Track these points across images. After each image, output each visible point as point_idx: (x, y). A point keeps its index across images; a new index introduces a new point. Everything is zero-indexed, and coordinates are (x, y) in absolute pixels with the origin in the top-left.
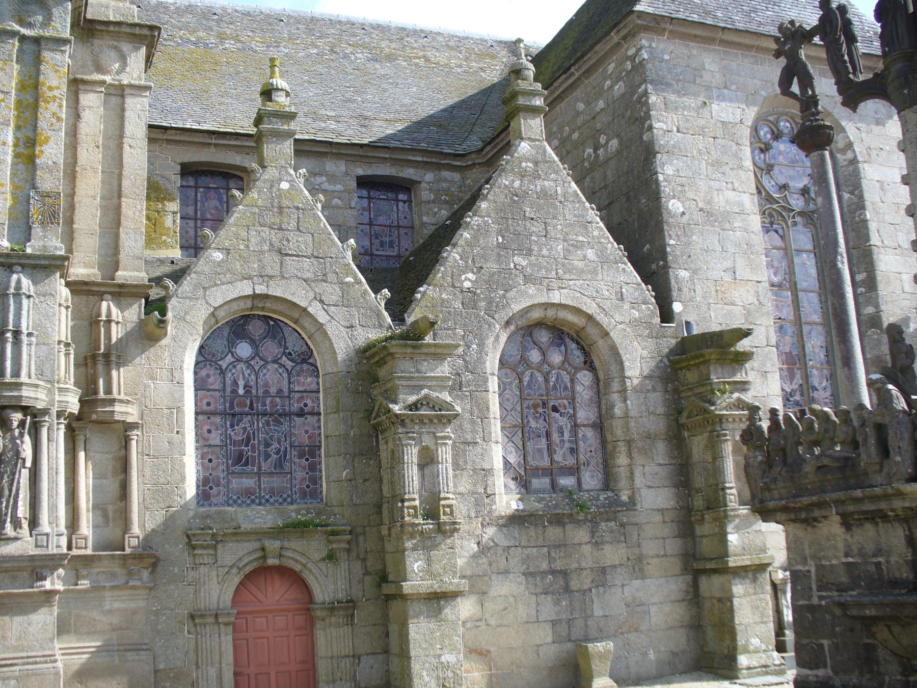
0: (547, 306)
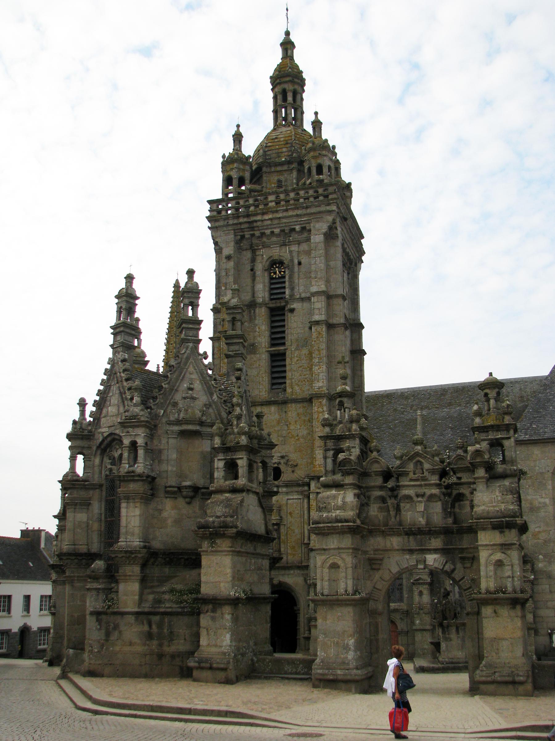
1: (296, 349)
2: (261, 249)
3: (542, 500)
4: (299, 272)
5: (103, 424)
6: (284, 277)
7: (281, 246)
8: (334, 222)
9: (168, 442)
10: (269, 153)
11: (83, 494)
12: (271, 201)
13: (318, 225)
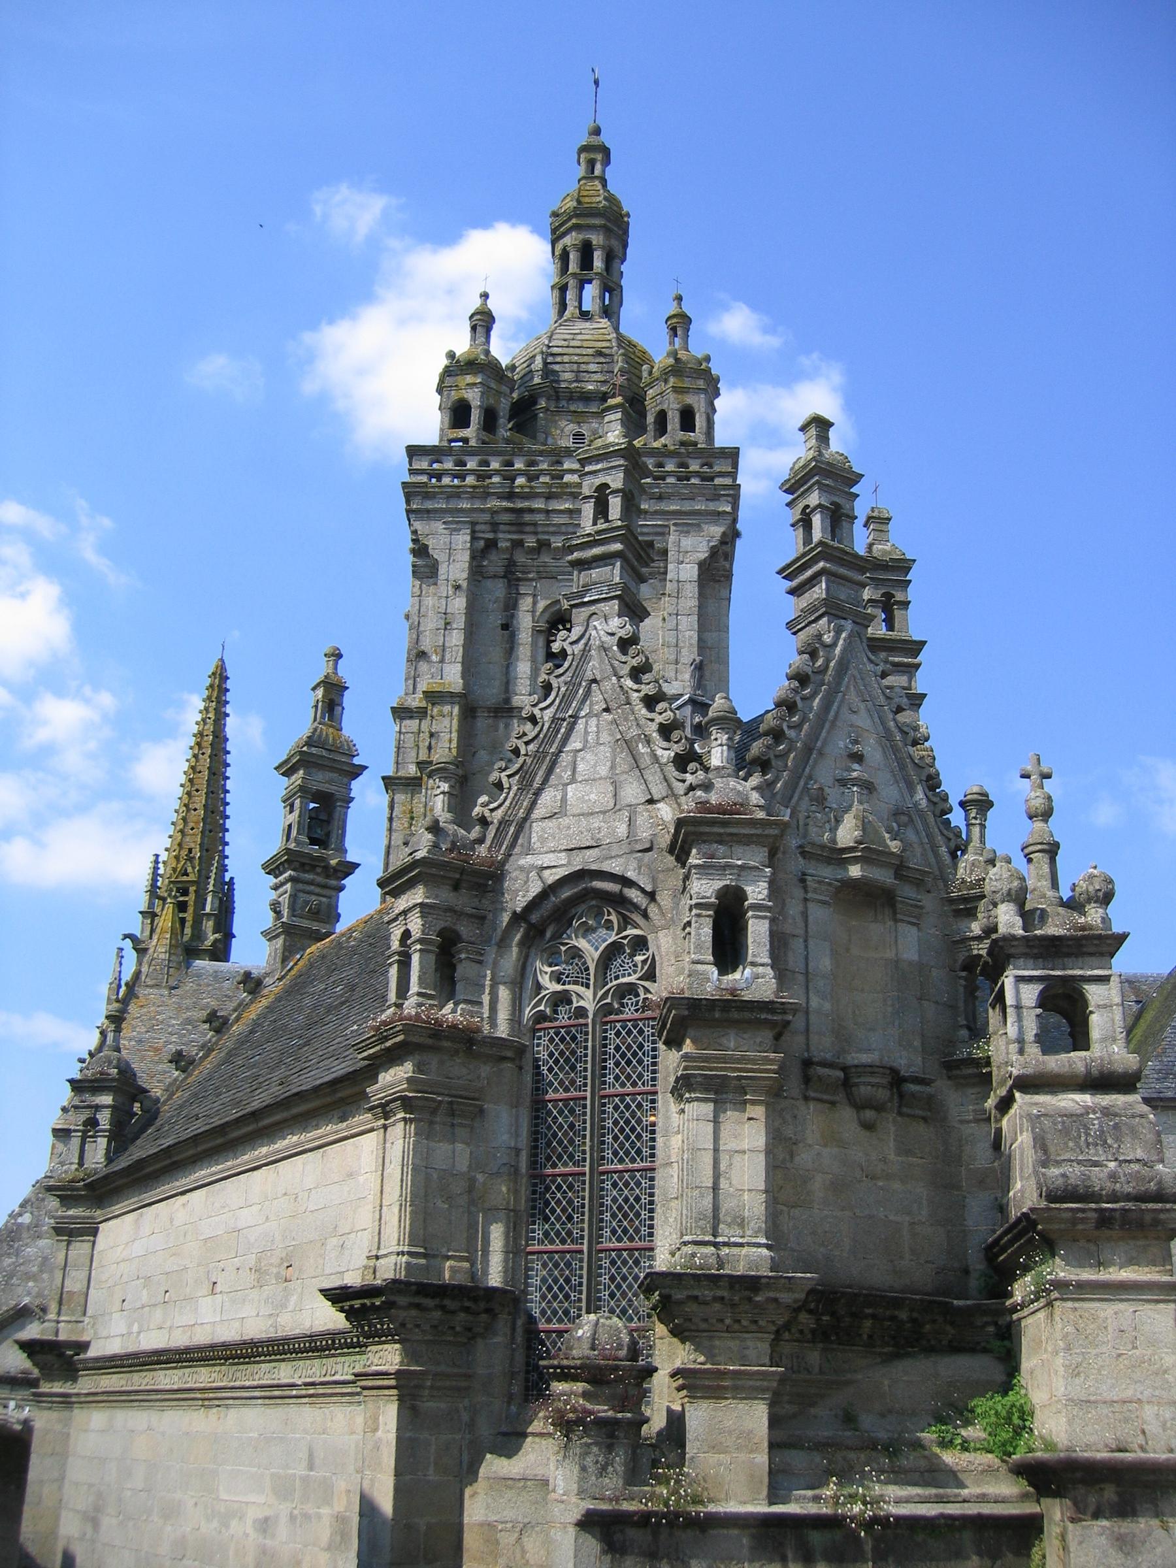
2: (532, 580)
5: (543, 840)
9: (805, 915)
10: (557, 367)
11: (459, 1071)
13: (687, 542)
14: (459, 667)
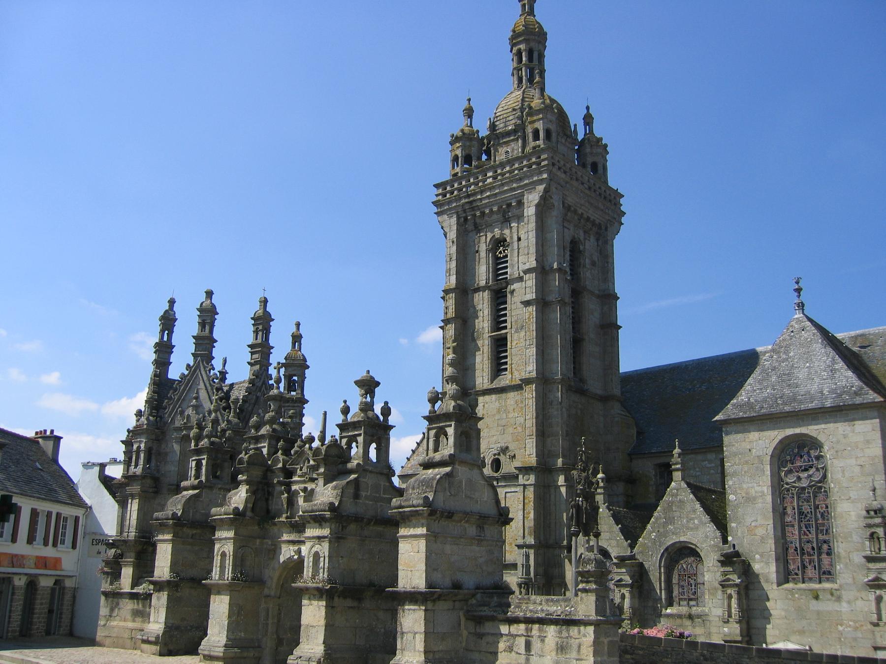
0: (680, 542)
1: (516, 332)
3: (758, 489)
4: (519, 249)
6: (506, 256)
7: (502, 223)
8: (546, 191)
12: (489, 177)
13: (531, 197)
14: (455, 276)
